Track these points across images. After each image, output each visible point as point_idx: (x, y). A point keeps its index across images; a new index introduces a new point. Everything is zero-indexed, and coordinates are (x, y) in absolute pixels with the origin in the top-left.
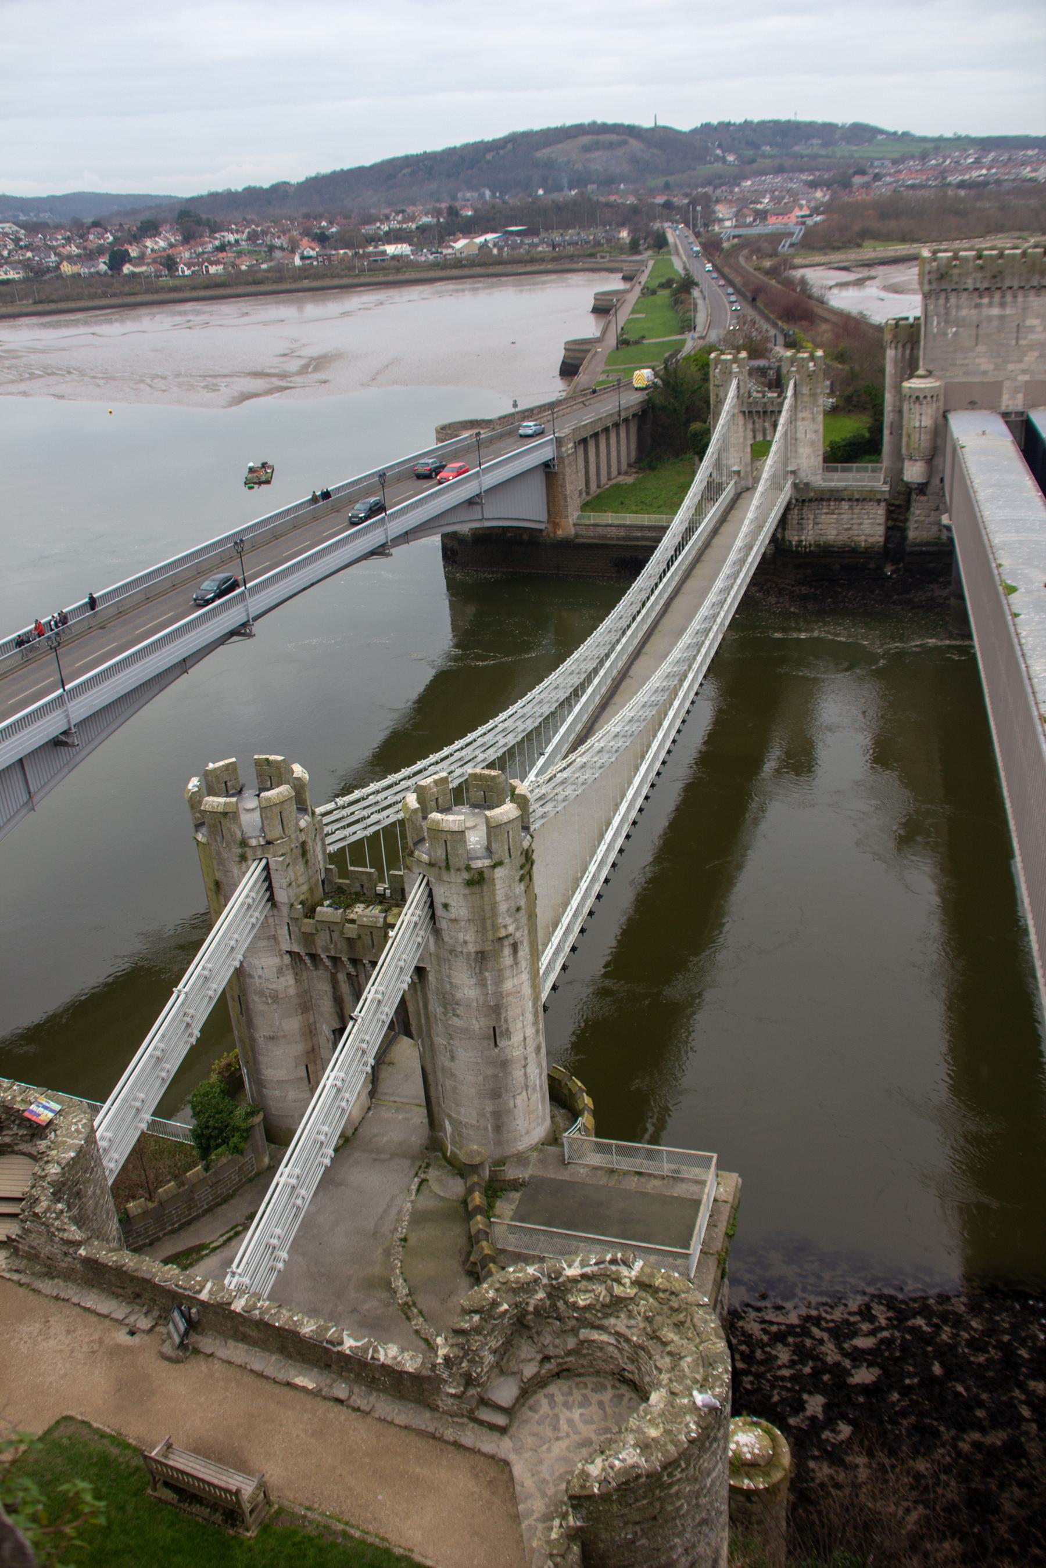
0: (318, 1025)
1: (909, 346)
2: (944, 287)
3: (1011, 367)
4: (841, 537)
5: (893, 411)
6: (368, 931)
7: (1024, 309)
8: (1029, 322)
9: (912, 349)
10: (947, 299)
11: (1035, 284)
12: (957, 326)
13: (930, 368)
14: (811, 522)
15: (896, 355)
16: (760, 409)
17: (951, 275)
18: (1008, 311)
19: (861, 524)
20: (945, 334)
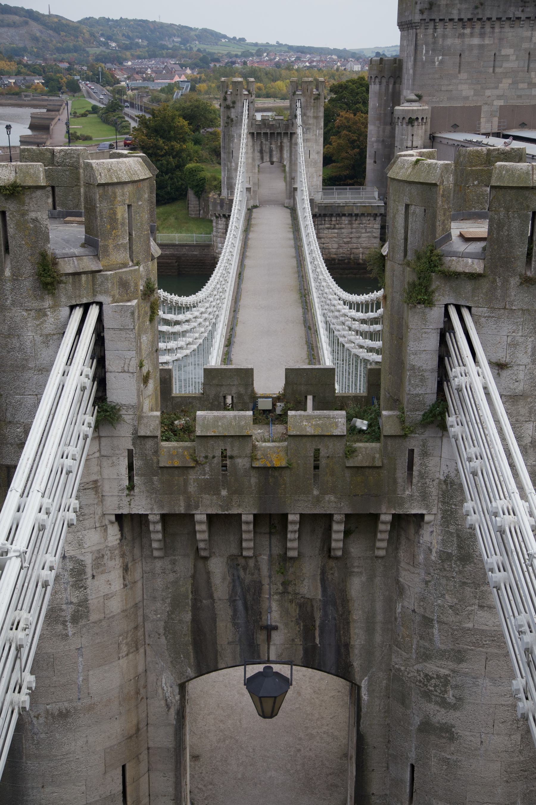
0: (152, 678)
1: (392, 81)
2: (433, 18)
3: (488, 93)
4: (341, 250)
5: (377, 141)
6: (309, 448)
7: (501, 39)
8: (504, 52)
9: (395, 83)
10: (435, 28)
11: (511, 16)
12: (443, 55)
13: (420, 93)
15: (380, 89)
16: (268, 131)
17: (439, 5)
18: (487, 41)
19: (359, 237)
20: (434, 62)
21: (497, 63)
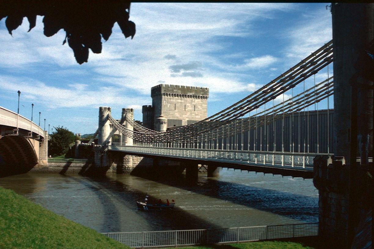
3: (184, 116)
8: (187, 105)
12: (170, 104)
14: (132, 159)
21: (186, 108)
